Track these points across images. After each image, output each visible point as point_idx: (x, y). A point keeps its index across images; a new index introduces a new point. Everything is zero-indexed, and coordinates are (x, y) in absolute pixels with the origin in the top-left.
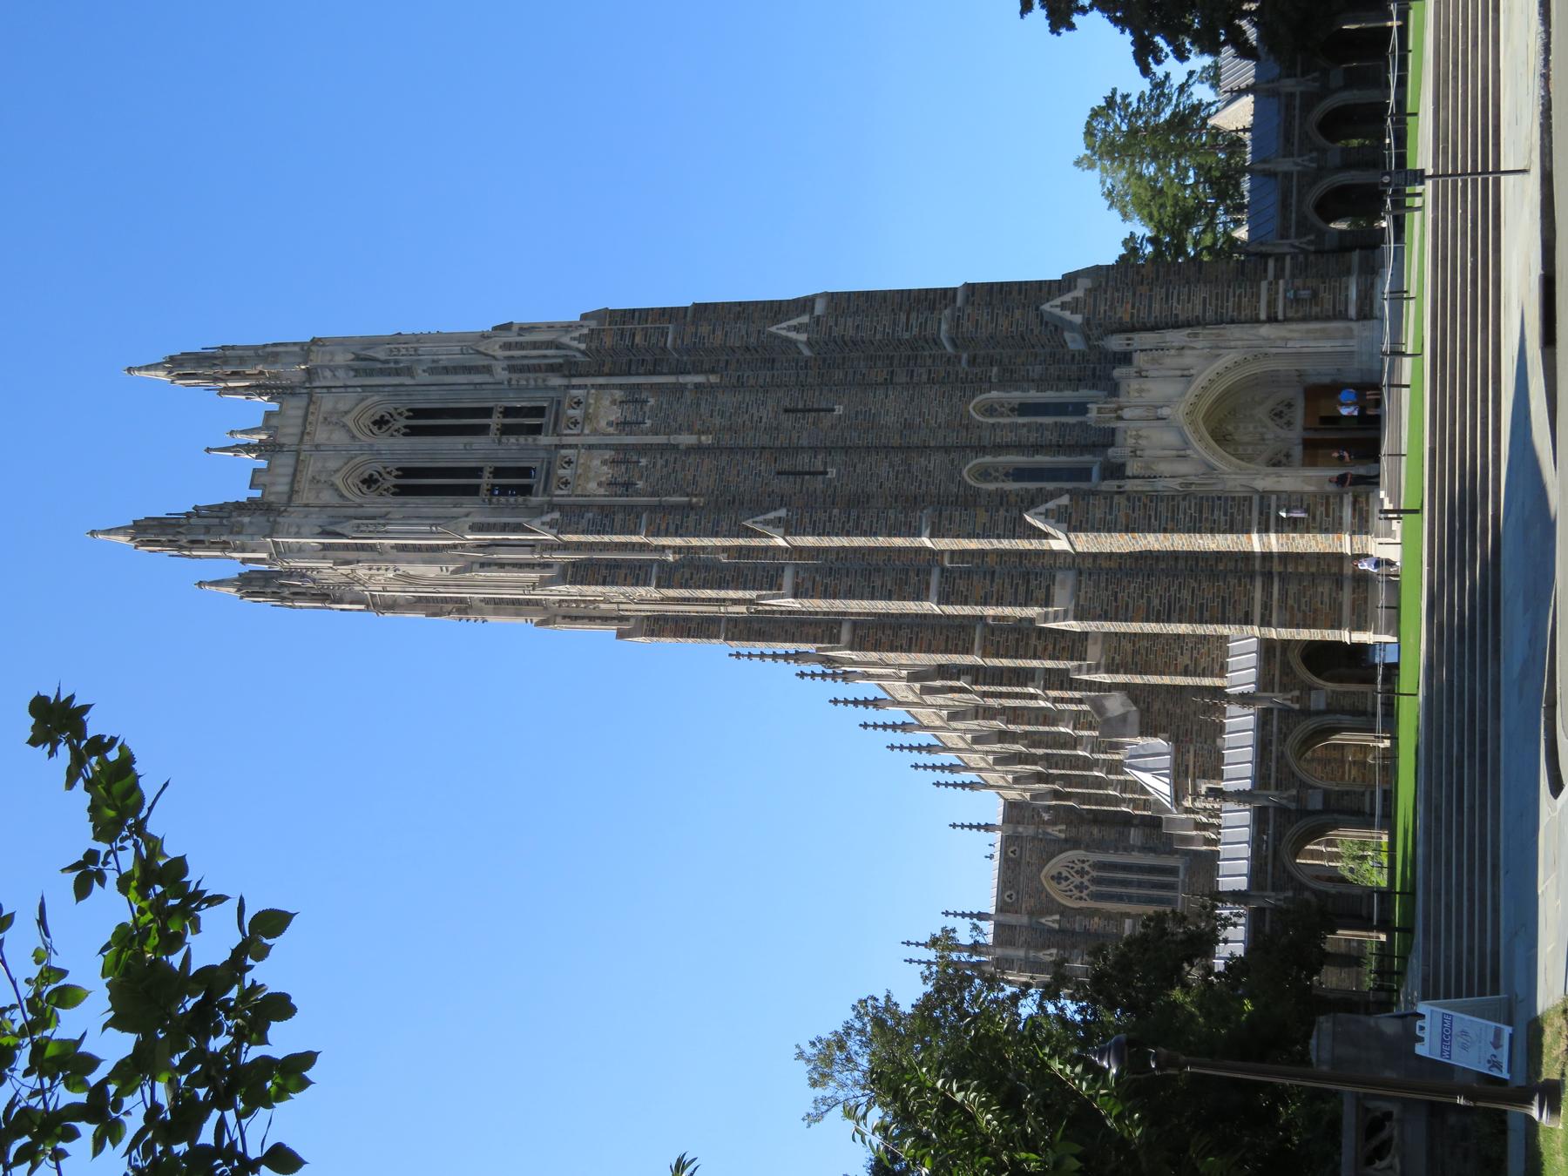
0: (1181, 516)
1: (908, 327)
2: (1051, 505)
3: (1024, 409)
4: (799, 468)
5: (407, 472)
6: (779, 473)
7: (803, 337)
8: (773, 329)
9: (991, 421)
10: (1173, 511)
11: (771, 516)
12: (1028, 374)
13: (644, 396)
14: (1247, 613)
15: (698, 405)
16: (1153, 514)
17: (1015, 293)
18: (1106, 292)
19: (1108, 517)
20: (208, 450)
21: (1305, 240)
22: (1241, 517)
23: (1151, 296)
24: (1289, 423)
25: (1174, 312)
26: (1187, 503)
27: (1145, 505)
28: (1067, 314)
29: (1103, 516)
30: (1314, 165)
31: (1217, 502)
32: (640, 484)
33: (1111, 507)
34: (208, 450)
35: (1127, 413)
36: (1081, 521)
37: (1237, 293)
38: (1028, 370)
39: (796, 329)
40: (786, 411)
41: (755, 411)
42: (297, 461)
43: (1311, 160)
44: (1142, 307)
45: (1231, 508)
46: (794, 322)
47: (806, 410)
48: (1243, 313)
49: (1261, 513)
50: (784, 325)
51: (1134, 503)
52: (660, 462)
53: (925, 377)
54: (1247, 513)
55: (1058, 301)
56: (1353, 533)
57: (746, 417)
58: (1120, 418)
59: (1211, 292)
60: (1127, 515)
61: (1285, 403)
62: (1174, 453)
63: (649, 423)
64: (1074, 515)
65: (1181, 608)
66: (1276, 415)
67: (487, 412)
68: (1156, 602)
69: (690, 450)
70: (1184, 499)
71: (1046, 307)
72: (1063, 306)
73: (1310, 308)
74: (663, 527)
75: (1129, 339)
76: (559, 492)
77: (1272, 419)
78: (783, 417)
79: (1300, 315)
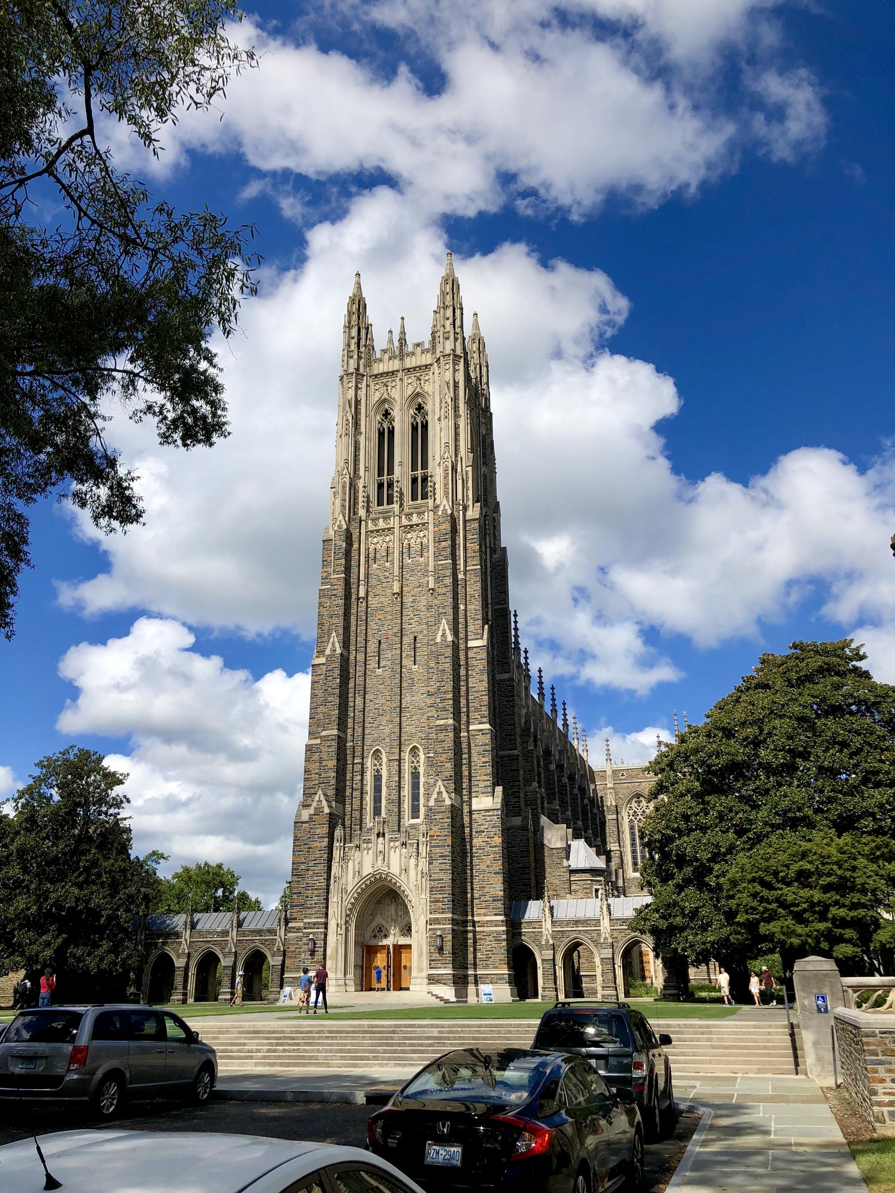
0: (315, 878)
1: (443, 700)
2: (325, 803)
3: (415, 775)
4: (382, 652)
5: (391, 432)
6: (380, 642)
7: (438, 640)
8: (444, 621)
9: (407, 758)
11: (337, 645)
13: (425, 554)
14: (295, 919)
15: (419, 587)
17: (484, 760)
20: (403, 318)
21: (549, 937)
28: (435, 796)
30: (602, 941)
32: (375, 566)
34: (403, 318)
35: (381, 839)
39: (444, 635)
40: (415, 638)
41: (416, 619)
42: (393, 372)
43: (606, 938)
46: (448, 632)
47: (415, 648)
49: (315, 924)
50: (446, 627)
52: (387, 574)
53: (430, 714)
55: (443, 789)
56: (454, 975)
57: (412, 616)
58: (378, 835)
63: (410, 561)
65: (299, 881)
67: (425, 466)
68: (303, 867)
69: (392, 587)
71: (440, 783)
72: (440, 793)
74: (336, 587)
76: (370, 522)
78: (412, 637)
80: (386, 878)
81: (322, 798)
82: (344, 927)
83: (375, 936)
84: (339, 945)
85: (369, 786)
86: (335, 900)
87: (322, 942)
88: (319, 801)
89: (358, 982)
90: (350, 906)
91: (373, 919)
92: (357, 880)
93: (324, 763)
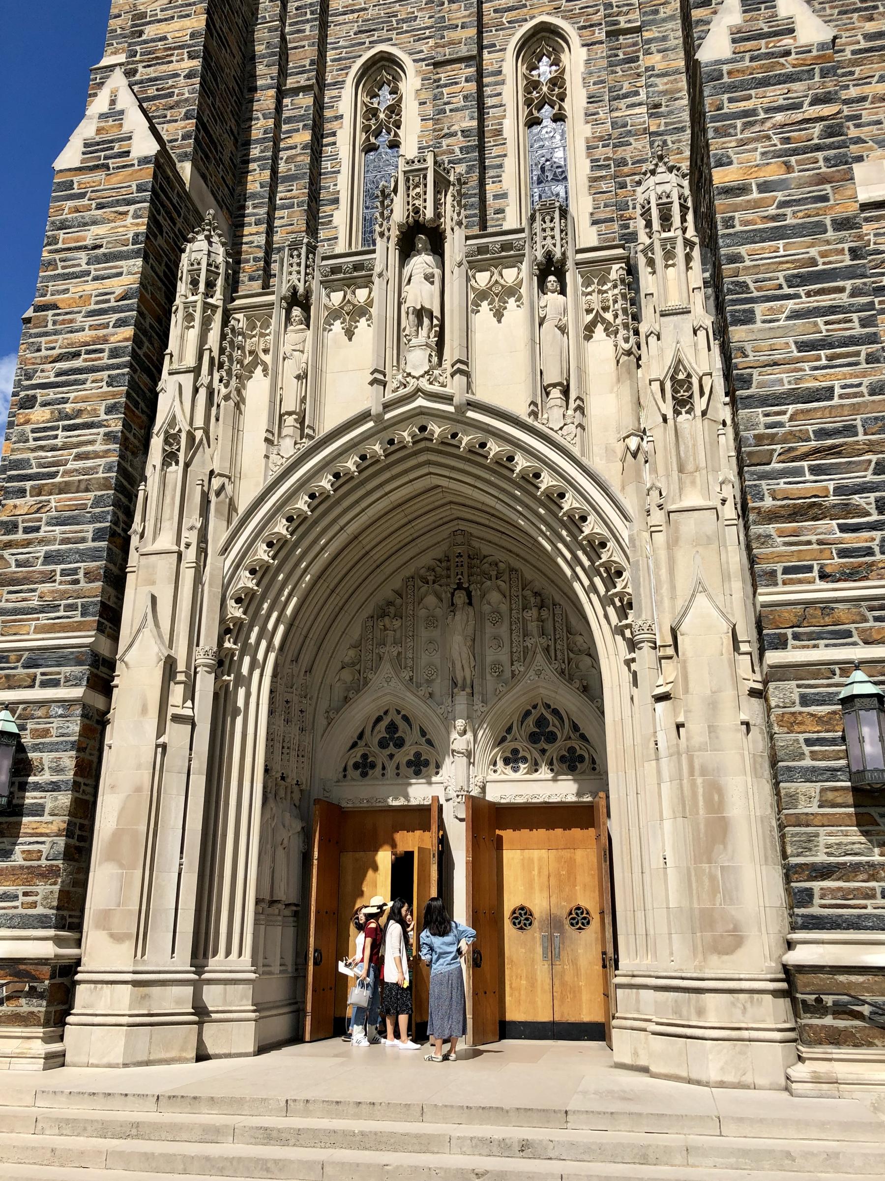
2: (136, 121)
9: (508, 67)
10: (79, 413)
12: (625, 96)
16: (77, 363)
18: (817, 101)
19: (83, 256)
22: (35, 603)
23: (818, 228)
24: (512, 760)
25: (760, 309)
26: (99, 447)
27: (105, 340)
29: (89, 242)
31: (89, 530)
33: (109, 258)
35: (422, 262)
36: (82, 196)
37: (856, 499)
38: (637, 93)
44: (772, 211)
45: (64, 573)
48: (771, 528)
51: (114, 310)
54: (44, 619)
59: (855, 409)
60: (84, 298)
61: (576, 744)
62: (290, 404)
64: (100, 175)
66: (541, 722)
70: (109, 437)
73: (811, 775)
75: (666, 219)
77: (528, 713)
79: (784, 739)
80: (449, 443)
81: (127, 101)
82: (205, 684)
83: (365, 766)
84: (174, 784)
85: (342, 183)
86: (166, 541)
87: (68, 760)
88: (115, 115)
89: (277, 989)
90: (246, 580)
91: (359, 685)
92: (288, 448)
93: (150, 32)
